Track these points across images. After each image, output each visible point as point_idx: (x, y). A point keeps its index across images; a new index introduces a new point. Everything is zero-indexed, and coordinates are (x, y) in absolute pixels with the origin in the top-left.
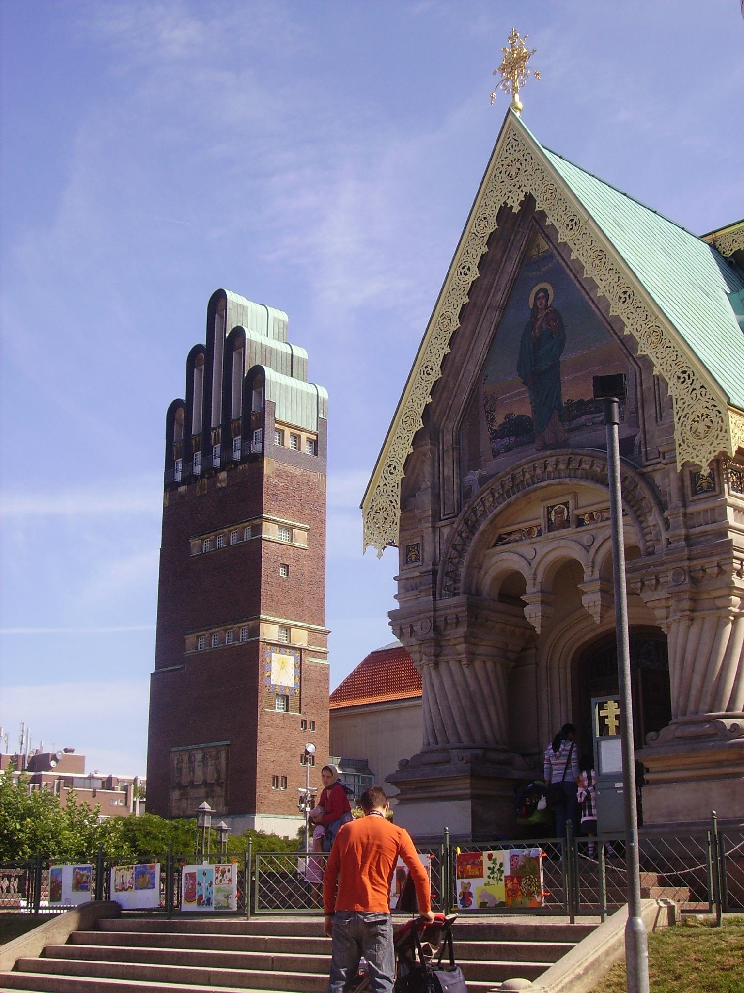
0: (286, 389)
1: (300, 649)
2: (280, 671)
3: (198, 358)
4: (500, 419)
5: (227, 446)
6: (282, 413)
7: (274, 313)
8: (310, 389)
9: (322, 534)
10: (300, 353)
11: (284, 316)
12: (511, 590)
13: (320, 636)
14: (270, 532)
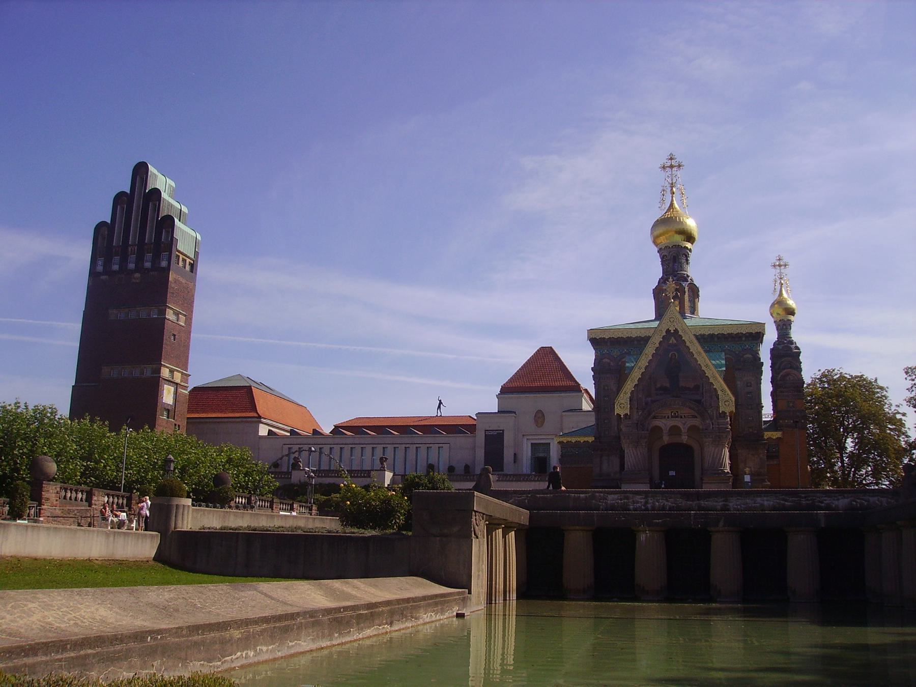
0: (183, 232)
1: (177, 384)
2: (168, 396)
3: (120, 199)
4: (659, 385)
5: (140, 259)
6: (181, 246)
7: (169, 181)
8: (193, 233)
9: (191, 319)
10: (185, 209)
11: (173, 185)
12: (658, 429)
13: (186, 377)
14: (170, 315)
